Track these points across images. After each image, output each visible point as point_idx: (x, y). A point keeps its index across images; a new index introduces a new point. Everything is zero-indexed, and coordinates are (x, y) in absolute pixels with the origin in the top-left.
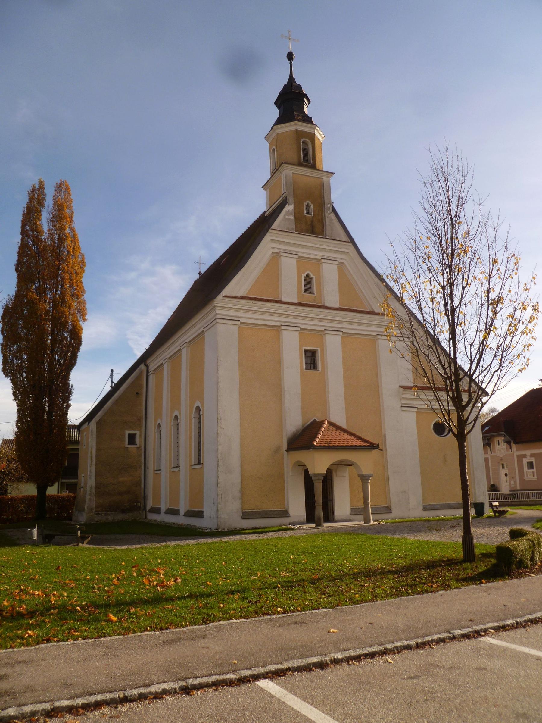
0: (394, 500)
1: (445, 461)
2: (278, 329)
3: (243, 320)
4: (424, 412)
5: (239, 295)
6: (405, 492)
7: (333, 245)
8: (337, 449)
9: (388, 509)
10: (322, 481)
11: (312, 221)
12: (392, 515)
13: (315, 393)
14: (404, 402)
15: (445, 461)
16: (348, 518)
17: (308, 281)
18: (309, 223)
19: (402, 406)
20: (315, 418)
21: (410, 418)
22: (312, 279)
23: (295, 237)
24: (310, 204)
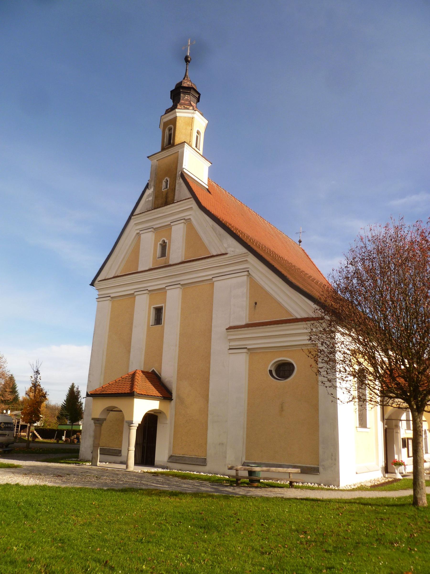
0: (211, 452)
1: (282, 409)
2: (132, 296)
3: (112, 295)
4: (284, 351)
5: (112, 276)
6: (223, 444)
7: (177, 207)
8: (116, 396)
9: (203, 462)
10: (136, 428)
11: (167, 194)
12: (207, 468)
13: (155, 347)
14: (233, 343)
15: (282, 409)
16: (165, 465)
17: (164, 246)
18: (164, 196)
19: (230, 349)
20: (153, 369)
21: (241, 361)
22: (166, 243)
23: (150, 214)
24: (169, 180)
